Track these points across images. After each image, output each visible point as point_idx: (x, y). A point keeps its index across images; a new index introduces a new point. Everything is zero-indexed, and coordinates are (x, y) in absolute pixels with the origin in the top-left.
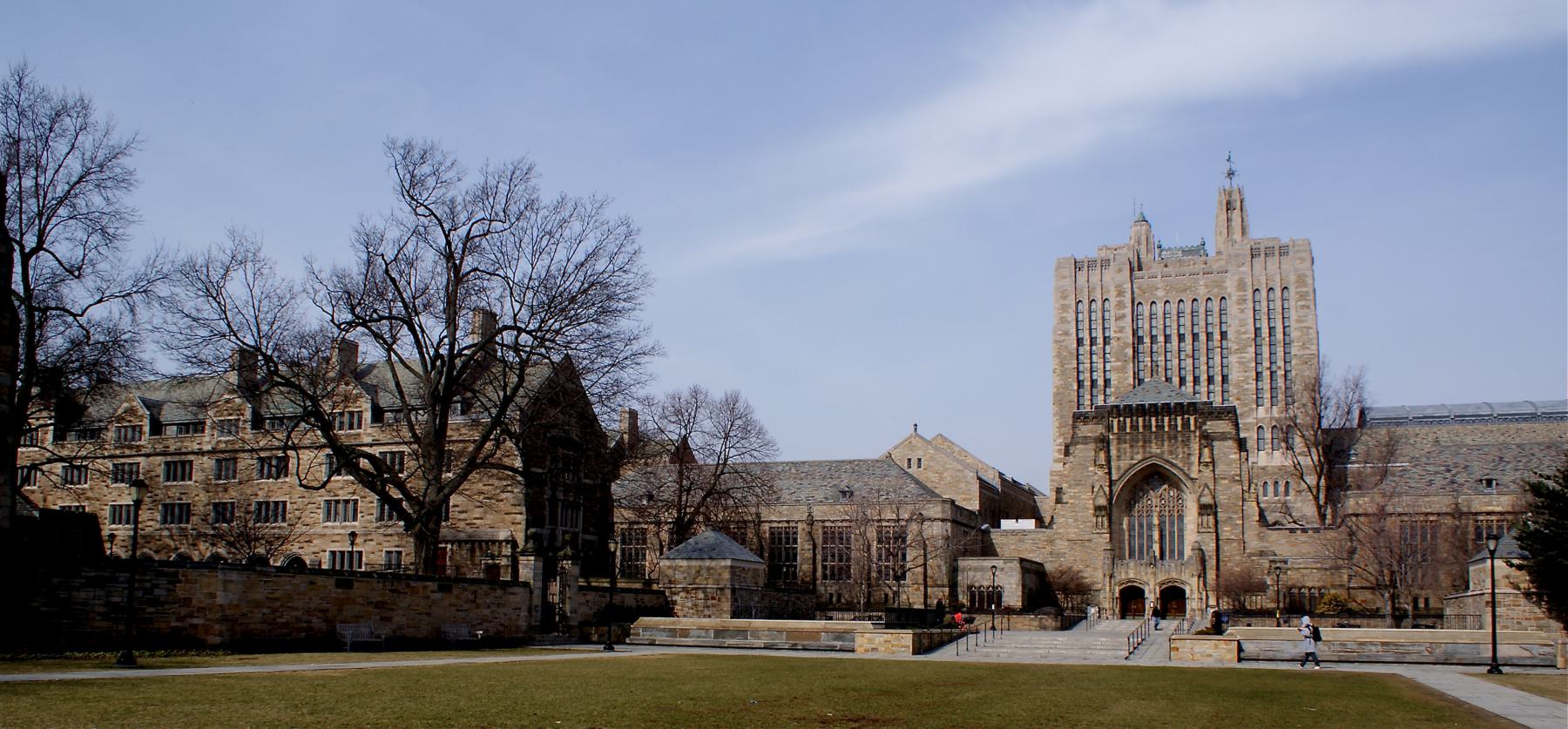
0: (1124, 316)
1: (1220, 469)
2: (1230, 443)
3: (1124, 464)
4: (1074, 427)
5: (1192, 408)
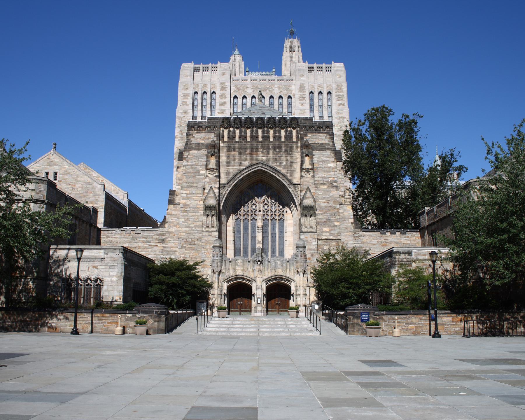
0: (225, 103)
1: (320, 175)
2: (328, 153)
3: (234, 169)
4: (188, 135)
5: (294, 122)
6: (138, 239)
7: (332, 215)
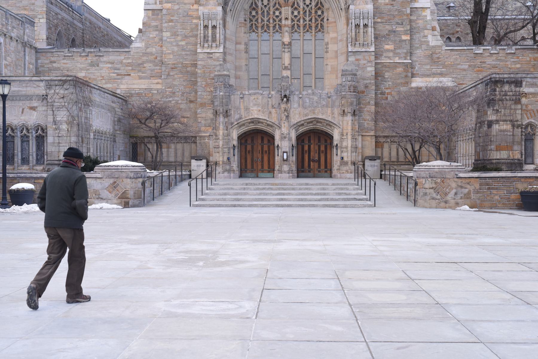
6: (101, 65)
7: (398, 23)
